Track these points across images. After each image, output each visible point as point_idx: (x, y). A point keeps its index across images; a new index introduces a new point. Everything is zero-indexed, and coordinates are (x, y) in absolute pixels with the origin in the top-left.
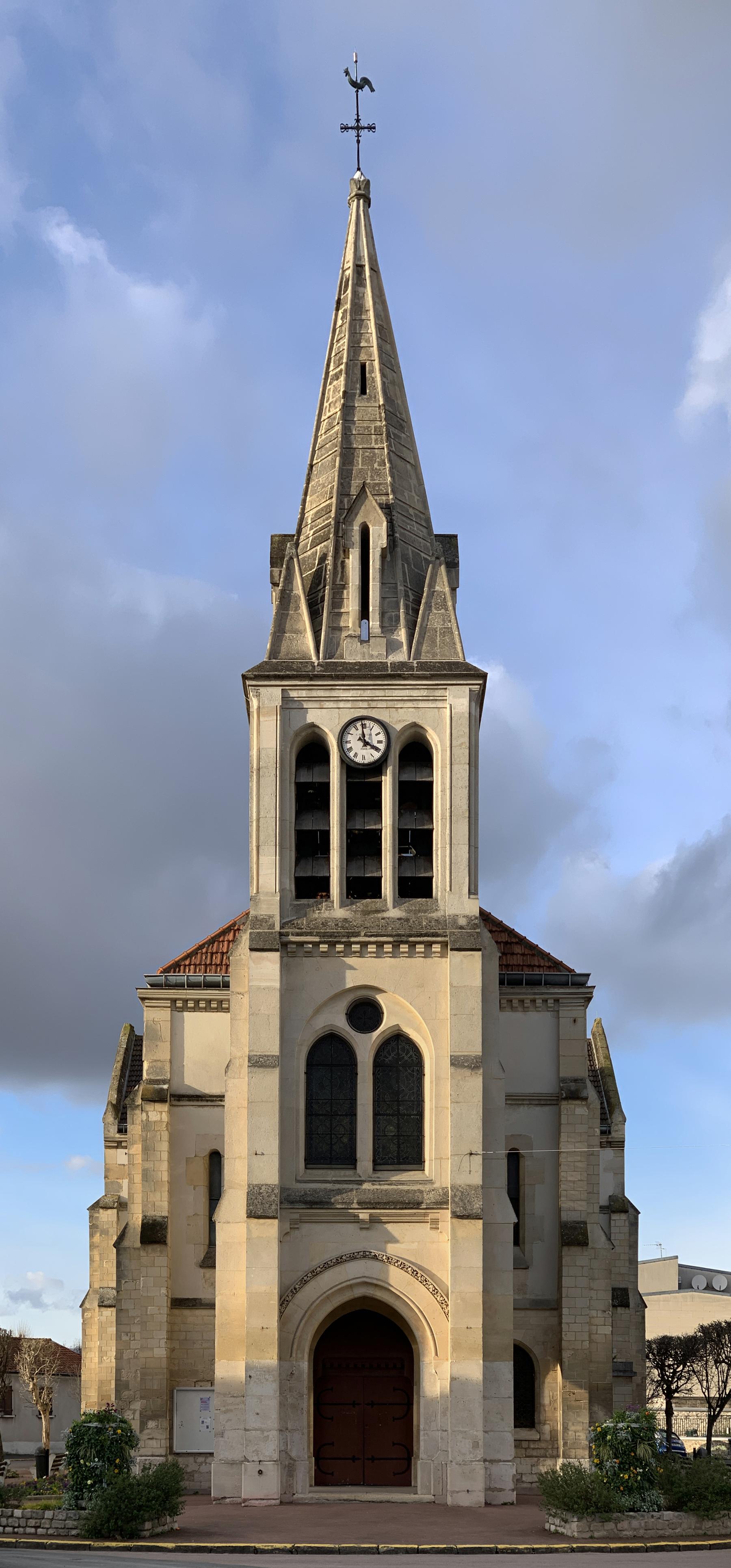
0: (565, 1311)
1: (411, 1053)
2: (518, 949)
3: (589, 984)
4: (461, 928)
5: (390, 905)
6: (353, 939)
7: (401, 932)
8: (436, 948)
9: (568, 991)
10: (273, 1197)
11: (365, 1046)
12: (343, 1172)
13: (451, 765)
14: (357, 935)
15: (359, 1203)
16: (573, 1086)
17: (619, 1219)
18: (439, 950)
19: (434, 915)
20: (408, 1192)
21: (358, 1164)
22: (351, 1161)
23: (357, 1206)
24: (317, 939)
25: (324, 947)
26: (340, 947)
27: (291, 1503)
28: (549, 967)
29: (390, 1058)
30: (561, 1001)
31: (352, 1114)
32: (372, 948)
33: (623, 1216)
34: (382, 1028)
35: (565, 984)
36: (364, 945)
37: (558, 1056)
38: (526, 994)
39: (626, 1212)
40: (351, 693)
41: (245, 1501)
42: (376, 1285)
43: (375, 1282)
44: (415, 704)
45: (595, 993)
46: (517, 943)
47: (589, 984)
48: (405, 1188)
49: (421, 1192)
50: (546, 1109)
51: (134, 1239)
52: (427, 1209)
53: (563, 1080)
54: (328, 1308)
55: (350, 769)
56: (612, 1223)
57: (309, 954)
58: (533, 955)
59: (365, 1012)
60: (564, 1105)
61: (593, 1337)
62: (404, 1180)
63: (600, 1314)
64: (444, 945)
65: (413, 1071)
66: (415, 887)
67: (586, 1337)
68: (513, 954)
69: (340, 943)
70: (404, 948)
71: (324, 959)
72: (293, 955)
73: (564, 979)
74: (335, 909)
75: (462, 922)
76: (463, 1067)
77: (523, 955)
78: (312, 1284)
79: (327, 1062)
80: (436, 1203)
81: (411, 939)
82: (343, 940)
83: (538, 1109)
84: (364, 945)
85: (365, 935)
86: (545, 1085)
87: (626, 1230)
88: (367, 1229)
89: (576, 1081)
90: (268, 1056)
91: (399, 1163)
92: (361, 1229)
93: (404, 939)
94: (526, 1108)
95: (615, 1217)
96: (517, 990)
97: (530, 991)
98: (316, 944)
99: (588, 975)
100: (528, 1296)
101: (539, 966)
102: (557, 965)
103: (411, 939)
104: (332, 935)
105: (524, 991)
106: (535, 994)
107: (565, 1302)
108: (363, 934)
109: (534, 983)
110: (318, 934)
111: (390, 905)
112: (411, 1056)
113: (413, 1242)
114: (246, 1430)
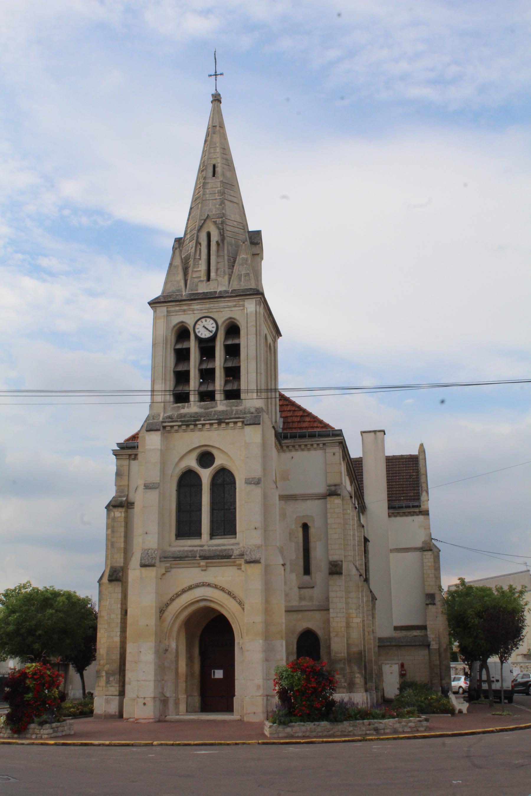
0: (331, 610)
2: (307, 419)
4: (252, 413)
5: (221, 405)
6: (197, 423)
7: (221, 417)
8: (240, 424)
9: (330, 439)
10: (154, 555)
11: (206, 475)
12: (194, 541)
14: (200, 420)
15: (200, 557)
16: (333, 488)
17: (428, 554)
18: (241, 425)
19: (240, 408)
20: (225, 550)
21: (203, 536)
24: (180, 424)
25: (184, 427)
26: (192, 427)
27: (165, 721)
28: (322, 427)
31: (200, 510)
32: (207, 426)
33: (430, 553)
35: (328, 436)
36: (203, 425)
38: (307, 442)
39: (431, 550)
41: (136, 720)
42: (211, 601)
46: (307, 416)
48: (223, 548)
49: (232, 549)
50: (323, 500)
51: (105, 580)
53: (329, 486)
54: (186, 613)
56: (424, 557)
57: (177, 431)
58: (315, 421)
59: (206, 458)
60: (329, 499)
61: (351, 624)
62: (222, 543)
63: (354, 611)
64: (243, 422)
66: (233, 395)
67: (344, 624)
68: (304, 422)
69: (191, 424)
70: (223, 425)
72: (169, 432)
73: (328, 433)
74: (193, 407)
75: (253, 410)
76: (251, 484)
77: (309, 422)
78: (177, 600)
80: (239, 555)
81: (227, 421)
82: (193, 423)
83: (316, 501)
84: (203, 425)
85: (204, 420)
86: (321, 489)
87: (432, 560)
88: (205, 570)
89: (335, 485)
90: (154, 483)
91: (224, 535)
92: (202, 570)
93: (223, 420)
94: (311, 501)
95: (425, 553)
96: (303, 440)
97: (310, 440)
98: (180, 426)
100: (314, 603)
101: (317, 427)
102: (326, 426)
103: (227, 421)
104: (188, 421)
105: (307, 440)
106: (312, 441)
107: (331, 606)
108: (202, 419)
109: (312, 436)
110: (181, 421)
111: (221, 405)
114: (138, 681)
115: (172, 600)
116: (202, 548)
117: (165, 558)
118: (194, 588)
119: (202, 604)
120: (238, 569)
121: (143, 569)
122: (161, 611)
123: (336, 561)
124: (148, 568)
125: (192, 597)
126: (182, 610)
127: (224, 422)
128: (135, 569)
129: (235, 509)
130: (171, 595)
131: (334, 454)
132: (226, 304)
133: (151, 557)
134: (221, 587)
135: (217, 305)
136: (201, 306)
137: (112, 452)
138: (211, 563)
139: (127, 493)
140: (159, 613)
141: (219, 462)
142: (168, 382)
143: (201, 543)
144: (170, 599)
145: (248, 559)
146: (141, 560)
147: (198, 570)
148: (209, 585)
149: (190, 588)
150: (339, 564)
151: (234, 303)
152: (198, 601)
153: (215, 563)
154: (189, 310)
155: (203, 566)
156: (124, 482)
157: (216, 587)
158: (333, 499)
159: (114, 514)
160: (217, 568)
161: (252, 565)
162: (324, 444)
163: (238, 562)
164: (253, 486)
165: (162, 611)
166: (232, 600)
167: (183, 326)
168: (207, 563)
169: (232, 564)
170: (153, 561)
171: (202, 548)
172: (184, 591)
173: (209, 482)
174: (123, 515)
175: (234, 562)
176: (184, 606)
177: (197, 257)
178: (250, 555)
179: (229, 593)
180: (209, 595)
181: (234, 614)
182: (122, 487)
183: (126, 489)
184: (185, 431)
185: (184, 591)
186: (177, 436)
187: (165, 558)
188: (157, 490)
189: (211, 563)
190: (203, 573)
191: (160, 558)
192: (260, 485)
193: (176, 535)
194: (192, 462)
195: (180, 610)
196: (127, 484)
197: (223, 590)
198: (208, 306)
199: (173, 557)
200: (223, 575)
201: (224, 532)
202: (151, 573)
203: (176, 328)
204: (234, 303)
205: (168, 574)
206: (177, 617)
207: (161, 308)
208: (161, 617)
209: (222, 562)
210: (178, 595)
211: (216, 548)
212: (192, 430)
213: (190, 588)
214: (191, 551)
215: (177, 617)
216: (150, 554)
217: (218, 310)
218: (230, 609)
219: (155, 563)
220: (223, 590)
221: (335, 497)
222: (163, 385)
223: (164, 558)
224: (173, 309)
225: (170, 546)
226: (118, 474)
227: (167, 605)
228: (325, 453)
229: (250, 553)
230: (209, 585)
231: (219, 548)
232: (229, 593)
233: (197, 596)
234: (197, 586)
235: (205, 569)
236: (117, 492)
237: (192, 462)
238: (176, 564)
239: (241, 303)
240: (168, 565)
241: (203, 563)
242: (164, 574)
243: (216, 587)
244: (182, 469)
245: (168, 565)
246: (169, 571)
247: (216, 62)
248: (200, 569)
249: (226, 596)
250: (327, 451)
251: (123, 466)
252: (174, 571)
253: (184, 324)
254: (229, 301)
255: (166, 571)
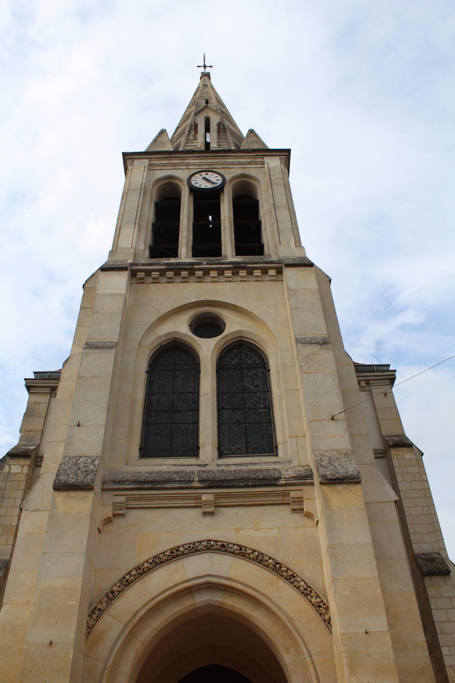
1: (254, 358)
3: (391, 368)
11: (207, 349)
13: (272, 186)
15: (200, 481)
20: (261, 470)
22: (194, 451)
23: (198, 485)
24: (164, 267)
29: (234, 363)
30: (371, 382)
32: (213, 274)
34: (225, 333)
37: (378, 420)
40: (197, 161)
43: (224, 582)
44: (243, 166)
45: (397, 374)
47: (391, 368)
52: (286, 485)
55: (196, 192)
59: (208, 325)
65: (257, 372)
71: (169, 285)
79: (171, 364)
85: (207, 264)
88: (212, 514)
92: (205, 514)
99: (389, 366)
108: (205, 263)
112: (254, 361)
113: (271, 529)
115: (126, 583)
116: (203, 468)
117: (115, 482)
118: (184, 555)
119: (201, 599)
120: (293, 510)
121: (61, 497)
122: (93, 612)
123: (429, 554)
124: (72, 494)
125: (178, 578)
126: (151, 610)
127: (244, 268)
128: (37, 510)
129: (269, 408)
130: (122, 573)
131: (385, 395)
132: (237, 160)
133: (84, 469)
134: (254, 551)
135: (222, 160)
136: (200, 161)
137: (24, 383)
138: (226, 496)
139: (38, 442)
140: (86, 618)
141: (233, 325)
142: (143, 232)
143: (200, 462)
144: (121, 581)
145: (328, 473)
146: (58, 475)
147: (193, 514)
148: (223, 548)
149: (175, 555)
150: (436, 558)
151: (249, 160)
152: (190, 591)
153: (237, 496)
154: (181, 164)
155: (207, 503)
156: (37, 425)
157: (241, 552)
158: (401, 452)
159: (10, 469)
160: (240, 510)
161: (340, 488)
162: (368, 383)
163: (292, 494)
164: (317, 348)
165: (95, 612)
166: (282, 584)
167: (171, 183)
168: (217, 496)
169: (279, 499)
170: (89, 477)
171: (203, 468)
172: (158, 562)
173: (215, 359)
174: (26, 470)
175: (285, 494)
176: (154, 602)
177: (191, 137)
178: (331, 468)
179: (277, 568)
180: (222, 574)
181: (291, 621)
182: (32, 434)
183: (39, 436)
184: (170, 281)
185: (158, 562)
186: (154, 287)
187: (115, 482)
188: (113, 351)
189: (226, 496)
190: (208, 520)
191: (104, 483)
192: (330, 346)
193: (140, 449)
194: (181, 327)
195: (143, 612)
196: (41, 429)
197: (259, 559)
198: (210, 161)
199: (136, 482)
200: (259, 526)
201: (247, 449)
202: (81, 506)
203: (160, 184)
204: (249, 160)
205: (119, 522)
206: (132, 634)
207: (141, 160)
208: (90, 628)
209: (254, 495)
210: (142, 571)
211: (239, 468)
212: (185, 280)
213: (175, 555)
214: (176, 473)
215: (132, 634)
216: (82, 465)
217: (224, 166)
218: (280, 608)
219: (93, 481)
220: (259, 559)
221: (404, 449)
222: (136, 230)
223: (114, 485)
224: (159, 162)
225: (127, 464)
226: (29, 414)
227: (112, 596)
228: (371, 395)
229: (331, 464)
230: (223, 548)
231: (244, 468)
232: (277, 568)
233: (191, 575)
234: (193, 549)
235: (212, 509)
236: (21, 440)
237: (181, 327)
238: (139, 499)
239: (259, 160)
240: (122, 499)
241: (207, 496)
242: (108, 521)
243: (241, 552)
244: (160, 337)
245: (122, 499)
246: (123, 515)
247: (204, 61)
248: (199, 511)
249: (267, 575)
250: (373, 391)
251: (39, 403)
252: (133, 515)
253: (172, 181)
254: (241, 157)
255: (114, 515)
